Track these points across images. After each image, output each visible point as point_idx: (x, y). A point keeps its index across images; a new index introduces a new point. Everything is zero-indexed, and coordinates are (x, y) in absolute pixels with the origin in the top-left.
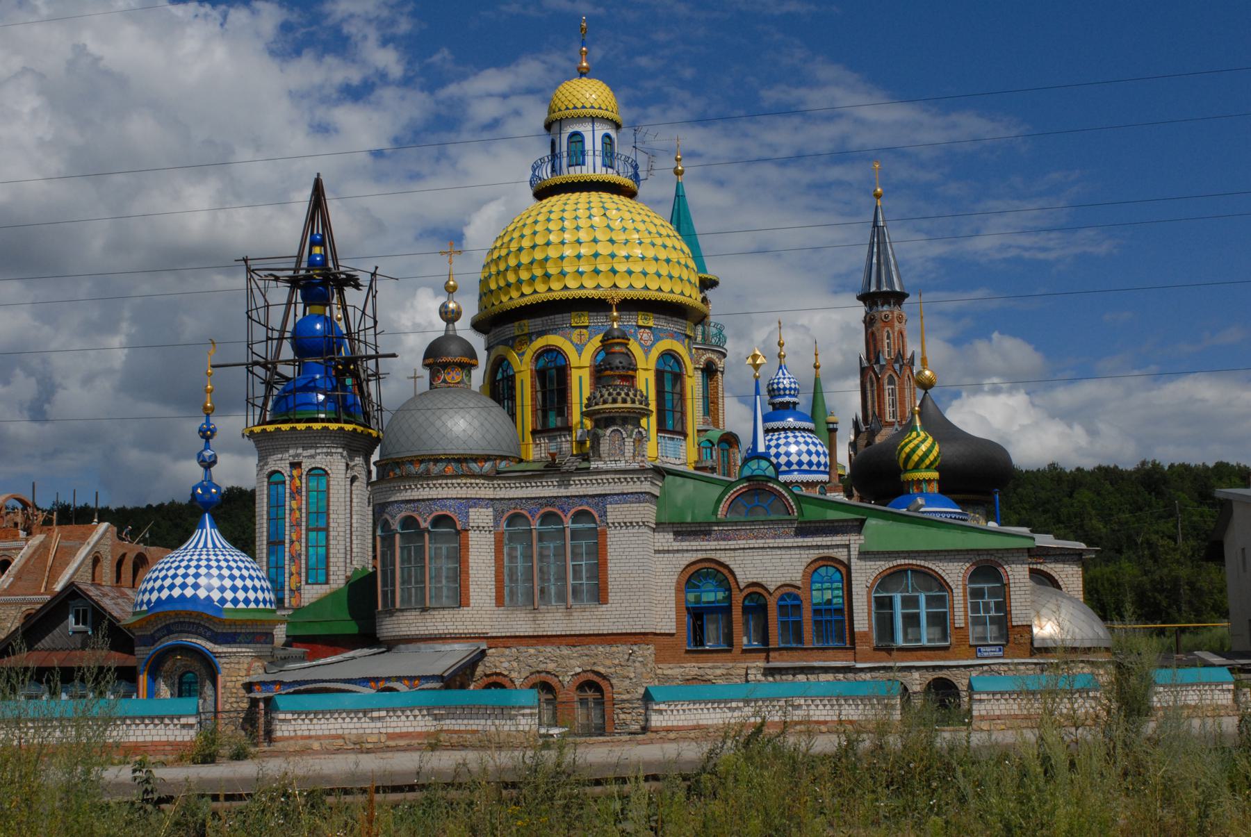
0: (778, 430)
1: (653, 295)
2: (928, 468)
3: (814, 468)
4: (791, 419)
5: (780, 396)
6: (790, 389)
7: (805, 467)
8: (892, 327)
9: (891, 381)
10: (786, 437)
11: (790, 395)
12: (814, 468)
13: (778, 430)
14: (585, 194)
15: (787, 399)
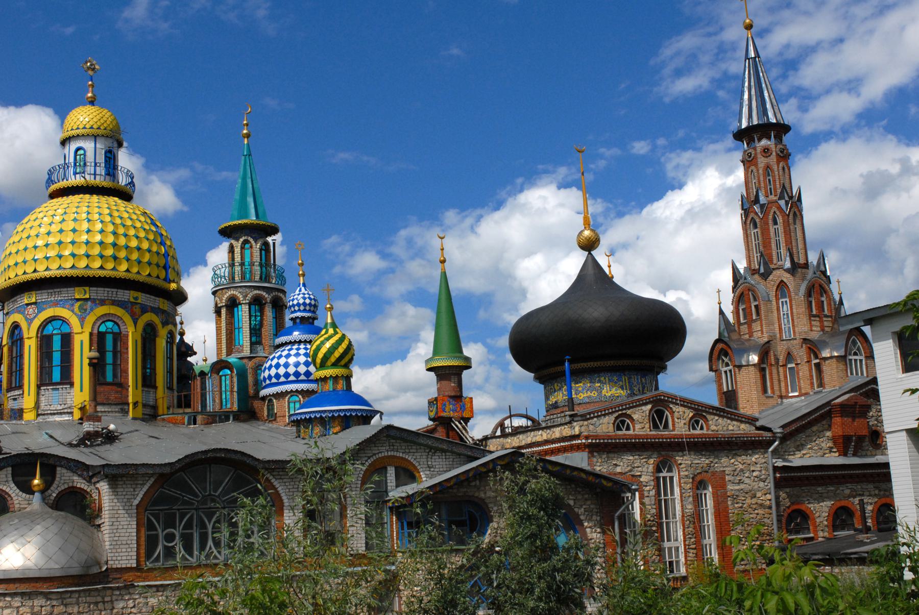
0: (286, 344)
1: (14, 281)
2: (335, 365)
3: (282, 379)
4: (296, 333)
5: (295, 311)
6: (299, 305)
7: (274, 380)
8: (756, 165)
9: (755, 227)
10: (298, 349)
11: (305, 310)
12: (282, 379)
13: (286, 344)
14: (88, 196)
15: (299, 314)
